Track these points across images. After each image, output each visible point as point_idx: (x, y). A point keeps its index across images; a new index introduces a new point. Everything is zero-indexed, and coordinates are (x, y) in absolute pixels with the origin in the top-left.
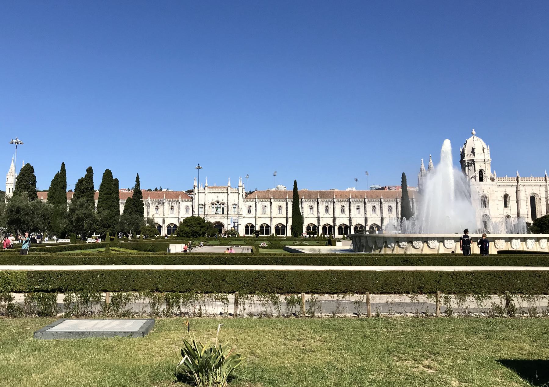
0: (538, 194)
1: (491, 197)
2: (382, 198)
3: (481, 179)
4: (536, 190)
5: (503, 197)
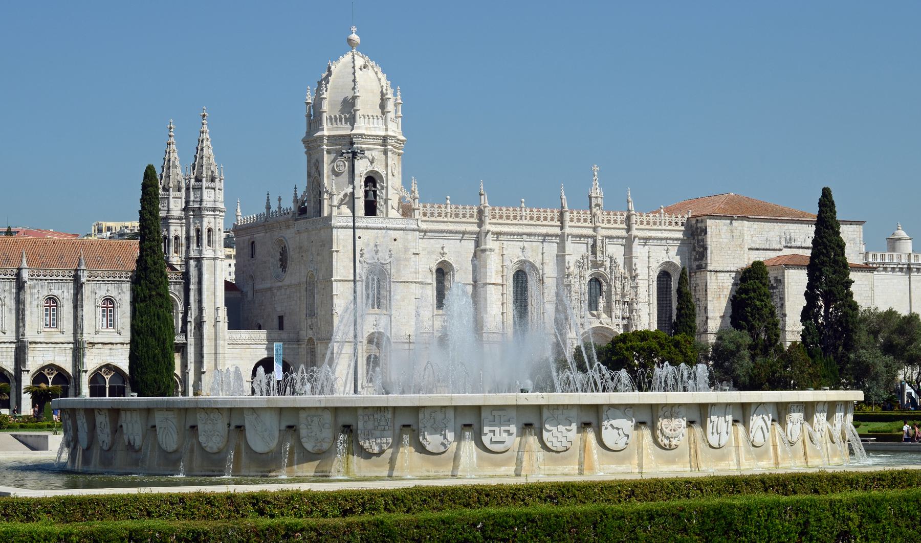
0: (538, 265)
1: (398, 271)
2: (25, 264)
3: (371, 209)
4: (534, 253)
5: (434, 271)
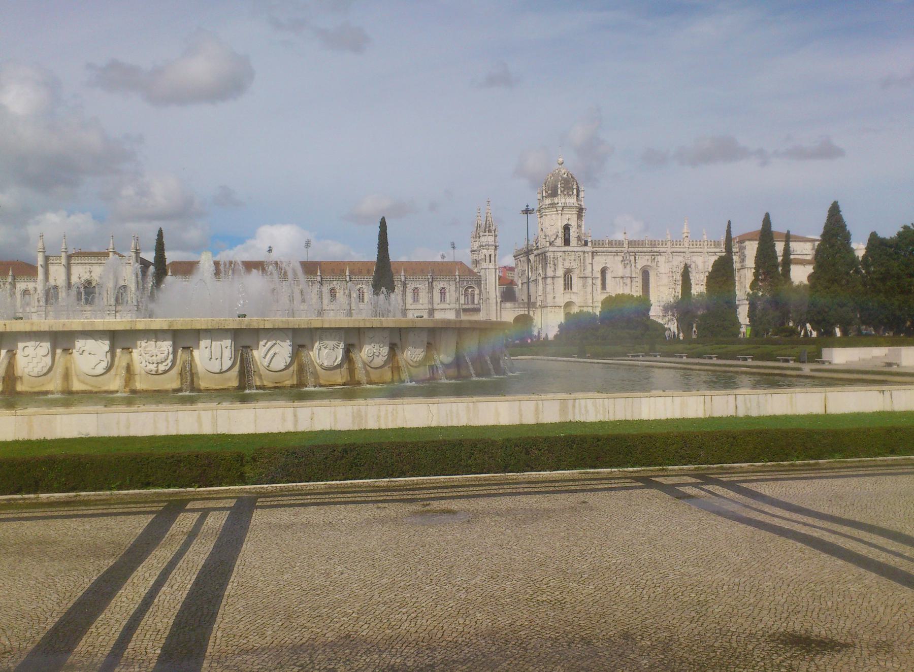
3: (567, 242)
